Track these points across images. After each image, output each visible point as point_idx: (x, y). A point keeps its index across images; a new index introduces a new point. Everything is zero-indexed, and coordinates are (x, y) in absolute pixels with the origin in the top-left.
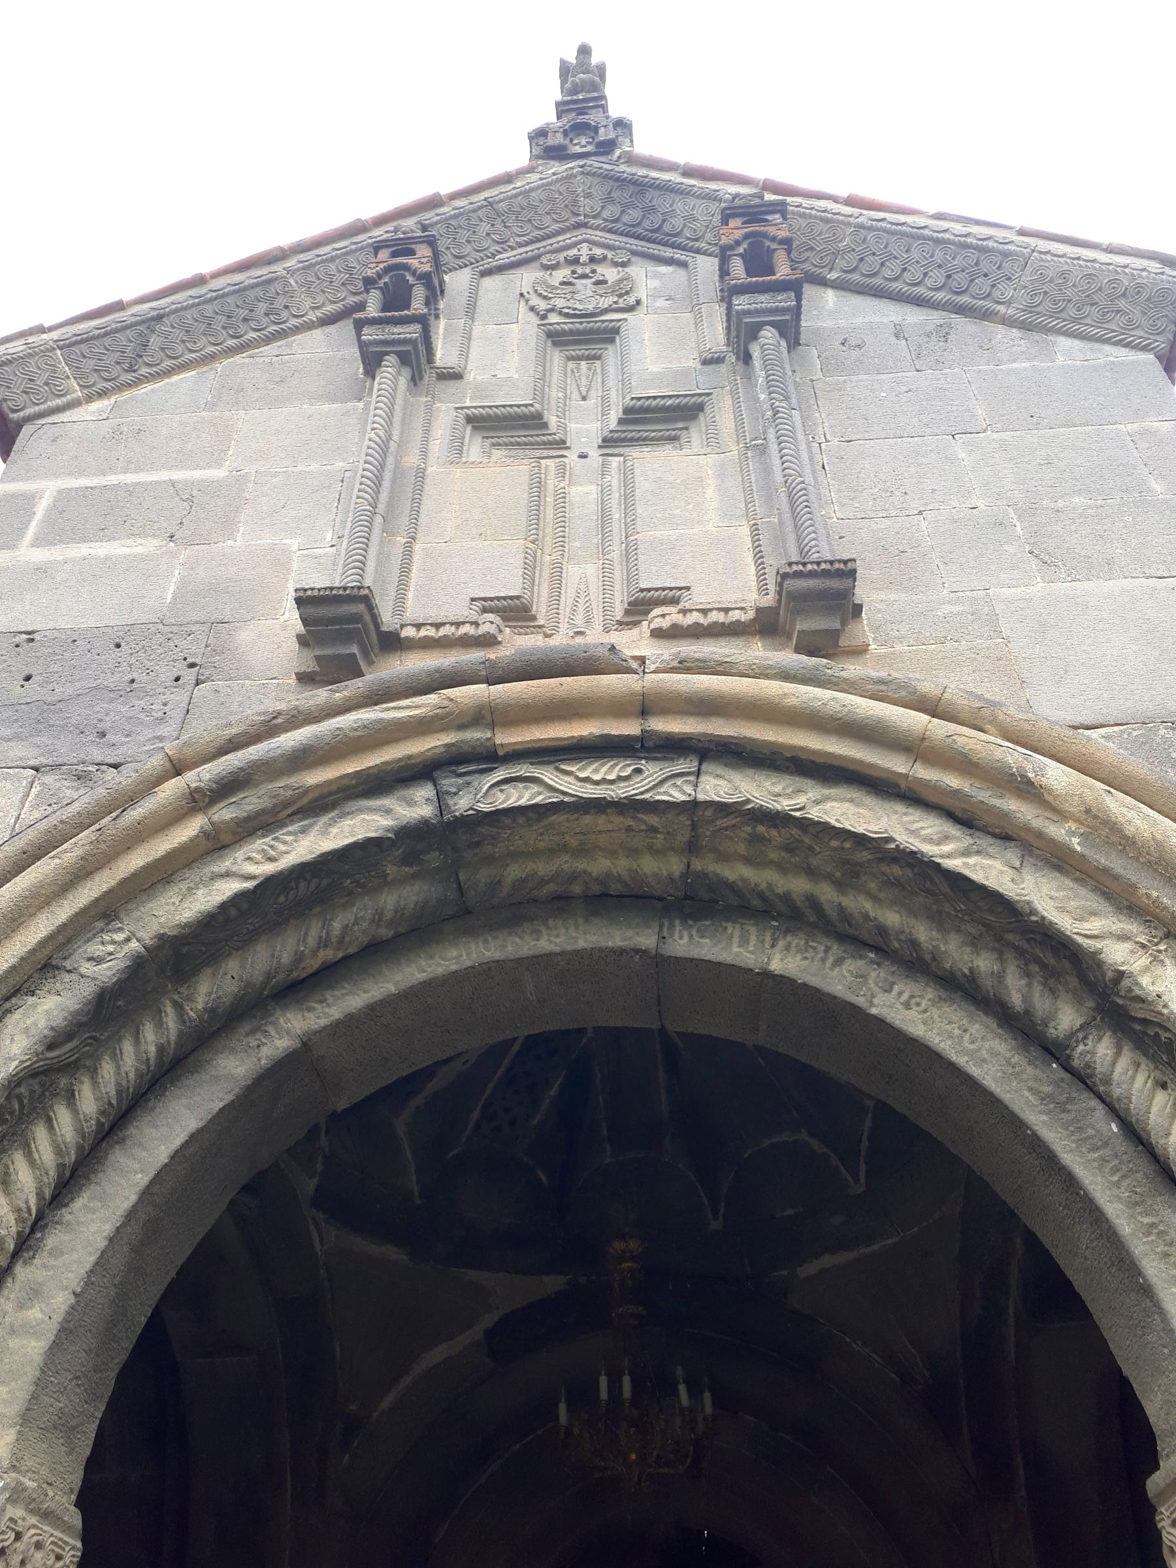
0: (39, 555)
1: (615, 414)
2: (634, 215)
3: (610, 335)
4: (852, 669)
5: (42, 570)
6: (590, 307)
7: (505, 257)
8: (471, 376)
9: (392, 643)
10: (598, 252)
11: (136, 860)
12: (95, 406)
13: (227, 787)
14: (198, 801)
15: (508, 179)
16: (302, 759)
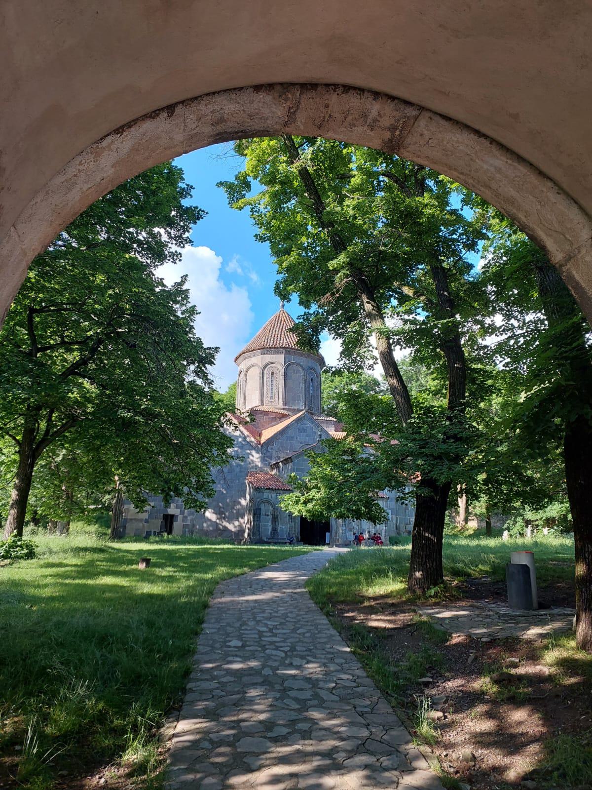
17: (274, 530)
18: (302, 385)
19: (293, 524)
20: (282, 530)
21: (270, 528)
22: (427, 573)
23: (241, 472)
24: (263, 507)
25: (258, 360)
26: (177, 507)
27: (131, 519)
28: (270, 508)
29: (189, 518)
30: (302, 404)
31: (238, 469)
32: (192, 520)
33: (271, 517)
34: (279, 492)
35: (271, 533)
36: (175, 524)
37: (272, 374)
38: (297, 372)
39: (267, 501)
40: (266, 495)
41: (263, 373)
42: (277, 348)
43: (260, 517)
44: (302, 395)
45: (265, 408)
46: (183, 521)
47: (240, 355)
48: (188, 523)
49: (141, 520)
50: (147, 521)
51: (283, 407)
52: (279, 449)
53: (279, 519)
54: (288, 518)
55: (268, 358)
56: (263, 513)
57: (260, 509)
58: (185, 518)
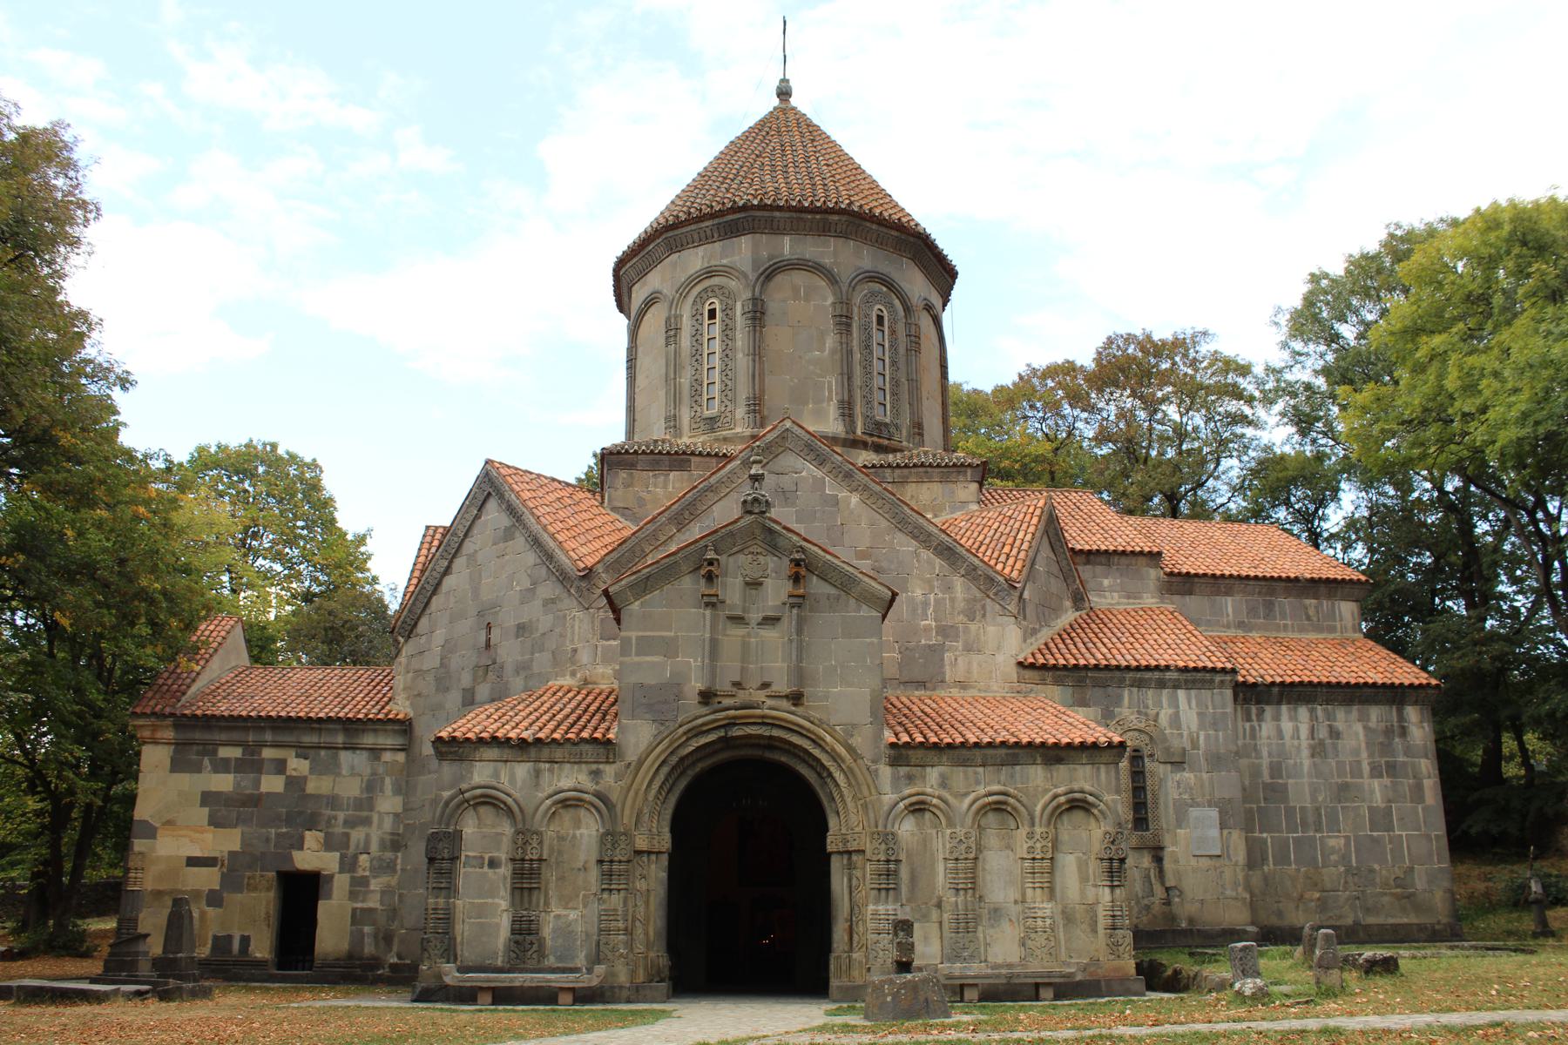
0: (637, 659)
1: (761, 615)
2: (769, 539)
3: (761, 584)
4: (799, 710)
5: (639, 664)
6: (756, 576)
7: (735, 549)
8: (728, 602)
9: (716, 695)
10: (759, 550)
11: (676, 745)
12: (637, 603)
13: (690, 730)
14: (685, 733)
15: (736, 521)
16: (703, 725)
17: (524, 931)
18: (831, 341)
19: (615, 900)
20: (565, 932)
21: (504, 923)
24: (469, 828)
26: (328, 845)
28: (507, 829)
29: (375, 885)
30: (832, 410)
33: (505, 870)
34: (546, 752)
35: (508, 950)
36: (323, 907)
37: (712, 314)
39: (489, 800)
40: (481, 773)
42: (721, 213)
43: (450, 875)
44: (832, 382)
45: (685, 441)
46: (353, 895)
48: (373, 902)
50: (214, 899)
51: (748, 432)
53: (550, 876)
54: (594, 873)
55: (695, 259)
56: (468, 852)
57: (458, 835)
58: (359, 886)
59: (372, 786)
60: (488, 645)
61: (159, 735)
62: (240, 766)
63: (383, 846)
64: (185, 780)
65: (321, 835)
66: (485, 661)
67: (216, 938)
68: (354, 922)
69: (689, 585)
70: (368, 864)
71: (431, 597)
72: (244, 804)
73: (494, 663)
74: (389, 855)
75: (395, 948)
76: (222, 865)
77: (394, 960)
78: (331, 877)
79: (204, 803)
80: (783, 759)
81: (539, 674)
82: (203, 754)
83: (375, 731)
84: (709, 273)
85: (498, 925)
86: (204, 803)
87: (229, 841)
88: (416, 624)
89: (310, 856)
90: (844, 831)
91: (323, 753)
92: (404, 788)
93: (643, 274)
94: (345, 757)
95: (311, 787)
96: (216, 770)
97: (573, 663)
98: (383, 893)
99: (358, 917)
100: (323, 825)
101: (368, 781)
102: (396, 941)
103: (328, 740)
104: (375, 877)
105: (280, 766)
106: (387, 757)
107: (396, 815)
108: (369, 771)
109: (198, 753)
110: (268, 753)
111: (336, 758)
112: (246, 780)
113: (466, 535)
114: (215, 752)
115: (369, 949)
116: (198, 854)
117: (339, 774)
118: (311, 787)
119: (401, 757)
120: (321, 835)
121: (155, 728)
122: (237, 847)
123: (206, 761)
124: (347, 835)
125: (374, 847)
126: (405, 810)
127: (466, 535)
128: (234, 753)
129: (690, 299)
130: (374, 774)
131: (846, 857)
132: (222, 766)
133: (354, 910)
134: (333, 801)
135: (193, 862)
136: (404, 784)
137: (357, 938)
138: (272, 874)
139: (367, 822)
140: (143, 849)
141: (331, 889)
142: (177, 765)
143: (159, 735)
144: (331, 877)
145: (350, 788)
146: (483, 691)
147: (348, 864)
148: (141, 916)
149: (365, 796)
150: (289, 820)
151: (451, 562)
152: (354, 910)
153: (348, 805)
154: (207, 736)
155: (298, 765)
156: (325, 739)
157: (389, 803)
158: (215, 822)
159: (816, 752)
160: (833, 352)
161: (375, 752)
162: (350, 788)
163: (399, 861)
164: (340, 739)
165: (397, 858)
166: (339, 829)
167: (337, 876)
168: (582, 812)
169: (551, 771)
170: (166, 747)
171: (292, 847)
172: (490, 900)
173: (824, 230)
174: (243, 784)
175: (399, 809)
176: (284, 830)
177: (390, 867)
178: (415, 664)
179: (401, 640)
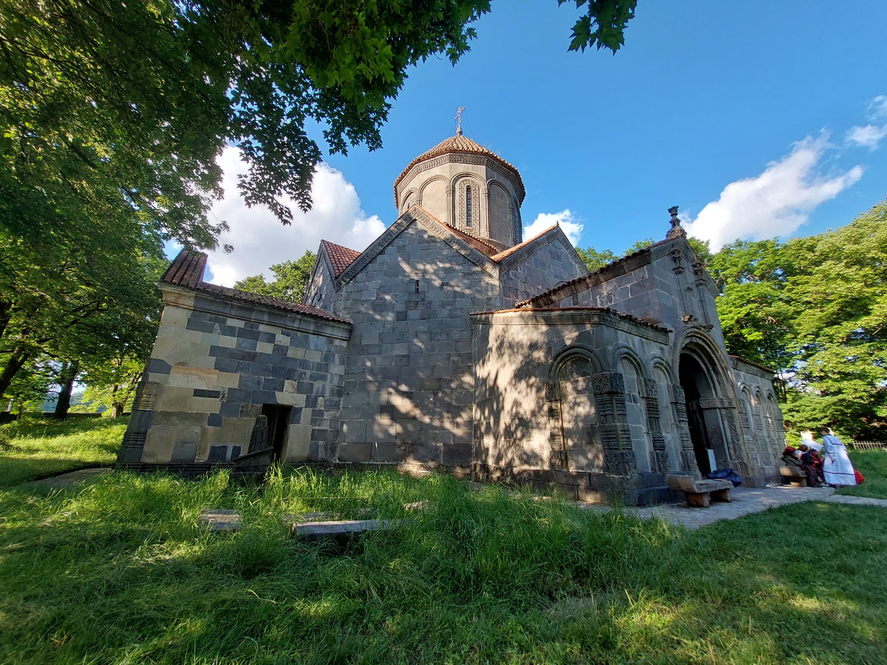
22: (540, 481)
23: (452, 317)
25: (445, 169)
26: (299, 390)
27: (167, 415)
31: (445, 312)
32: (334, 420)
38: (502, 197)
41: (454, 187)
46: (313, 422)
47: (410, 168)
48: (325, 426)
49: (198, 418)
50: (214, 420)
52: (526, 278)
55: (461, 168)
59: (328, 358)
60: (417, 291)
61: (181, 301)
62: (241, 333)
63: (332, 393)
64: (198, 336)
65: (295, 383)
66: (415, 298)
67: (213, 448)
68: (312, 440)
69: (667, 260)
70: (323, 404)
71: (368, 264)
72: (243, 358)
73: (423, 300)
74: (336, 399)
75: (337, 455)
76: (223, 397)
77: (337, 461)
78: (302, 408)
79: (211, 354)
80: (697, 358)
81: (461, 309)
82: (216, 320)
83: (333, 326)
84: (467, 175)
85: (644, 442)
86: (211, 354)
87: (230, 381)
88: (355, 277)
89: (287, 396)
90: (721, 397)
91: (299, 334)
92: (347, 361)
93: (427, 168)
94: (312, 337)
95: (290, 354)
96: (224, 333)
97: (488, 305)
98: (331, 421)
99: (315, 435)
100: (296, 377)
101: (326, 355)
102: (338, 450)
103: (304, 327)
104: (327, 411)
105: (271, 338)
106: (337, 342)
107: (340, 376)
108: (326, 349)
109: (210, 320)
110: (262, 328)
111: (307, 338)
112: (246, 344)
113: (396, 237)
114: (224, 322)
115: (321, 455)
116: (204, 387)
117: (309, 348)
118: (290, 354)
119: (345, 344)
120: (295, 383)
121: (179, 295)
122: (236, 386)
123: (217, 326)
124: (312, 385)
125: (327, 393)
126: (347, 373)
127: (396, 237)
128: (240, 324)
129: (458, 183)
130: (329, 351)
131: (724, 412)
132: (231, 331)
133: (313, 430)
134: (304, 364)
135: (198, 393)
136: (346, 359)
137: (315, 449)
138: (260, 406)
139: (324, 378)
140: (157, 381)
141: (300, 417)
142: (192, 325)
143: (181, 301)
144: (302, 408)
145: (315, 358)
146: (414, 314)
147: (311, 402)
148: (149, 431)
149: (323, 363)
150: (274, 372)
151: (385, 248)
152: (313, 430)
153: (313, 366)
154: (220, 309)
155: (282, 339)
156: (304, 326)
157: (336, 369)
158: (219, 367)
159: (713, 356)
160: (509, 220)
161: (330, 339)
162: (315, 358)
163: (341, 403)
164: (312, 328)
165: (340, 400)
166: (306, 381)
167: (304, 409)
168: (660, 372)
169: (647, 343)
170: (186, 311)
171: (275, 389)
172: (638, 425)
173: (507, 177)
174: (244, 345)
175: (343, 374)
176: (271, 378)
177: (336, 406)
178: (354, 296)
179: (344, 283)
